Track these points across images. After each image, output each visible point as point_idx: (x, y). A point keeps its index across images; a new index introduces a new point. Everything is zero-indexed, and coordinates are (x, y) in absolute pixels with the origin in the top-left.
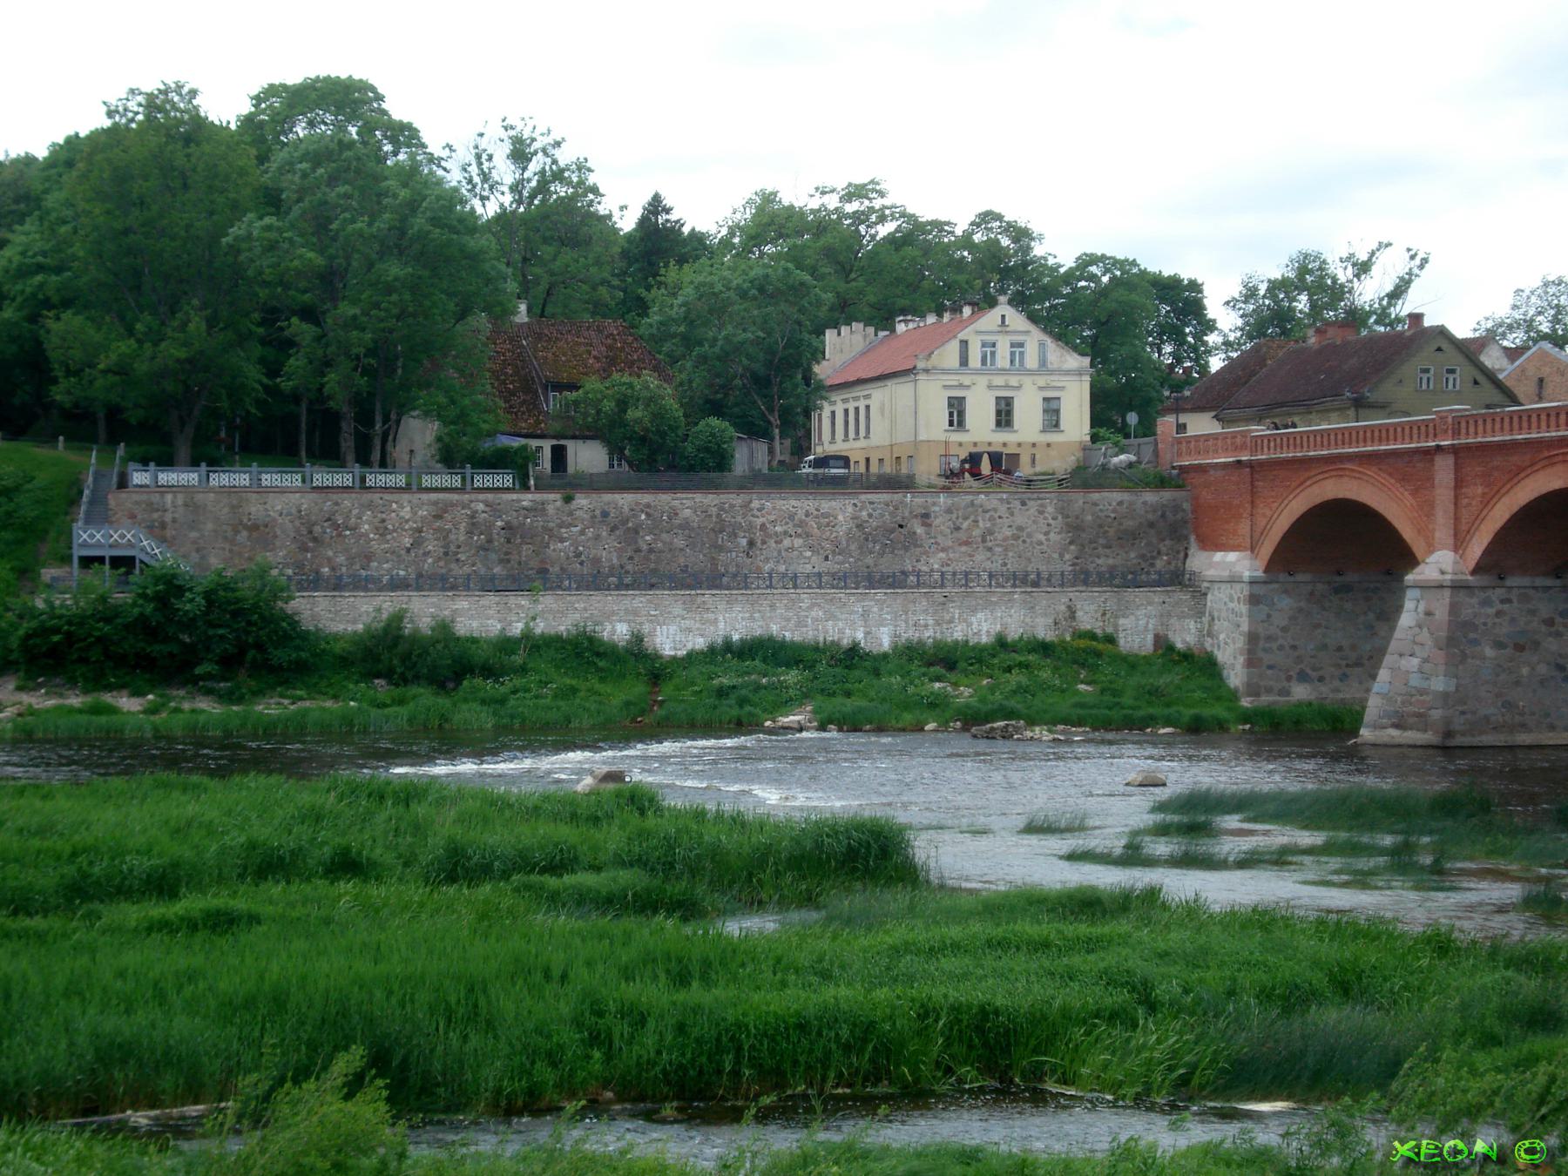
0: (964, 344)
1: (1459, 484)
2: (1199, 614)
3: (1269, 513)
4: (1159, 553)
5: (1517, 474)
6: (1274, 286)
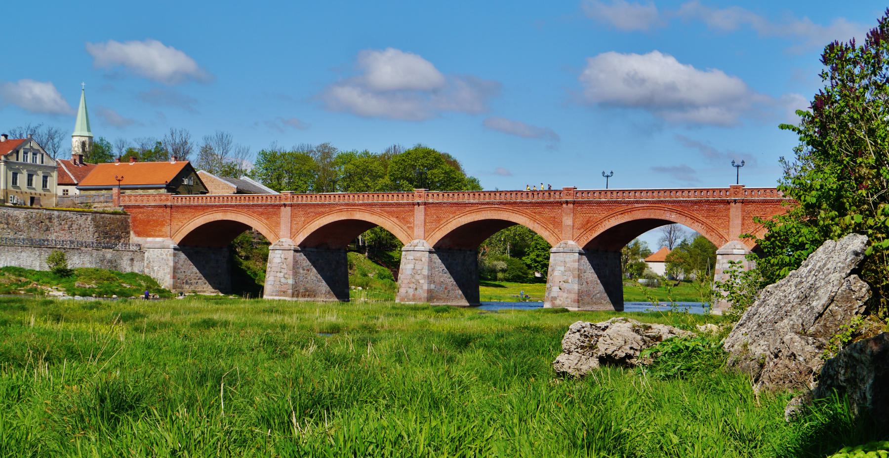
1: (292, 217)
2: (143, 260)
5: (322, 214)
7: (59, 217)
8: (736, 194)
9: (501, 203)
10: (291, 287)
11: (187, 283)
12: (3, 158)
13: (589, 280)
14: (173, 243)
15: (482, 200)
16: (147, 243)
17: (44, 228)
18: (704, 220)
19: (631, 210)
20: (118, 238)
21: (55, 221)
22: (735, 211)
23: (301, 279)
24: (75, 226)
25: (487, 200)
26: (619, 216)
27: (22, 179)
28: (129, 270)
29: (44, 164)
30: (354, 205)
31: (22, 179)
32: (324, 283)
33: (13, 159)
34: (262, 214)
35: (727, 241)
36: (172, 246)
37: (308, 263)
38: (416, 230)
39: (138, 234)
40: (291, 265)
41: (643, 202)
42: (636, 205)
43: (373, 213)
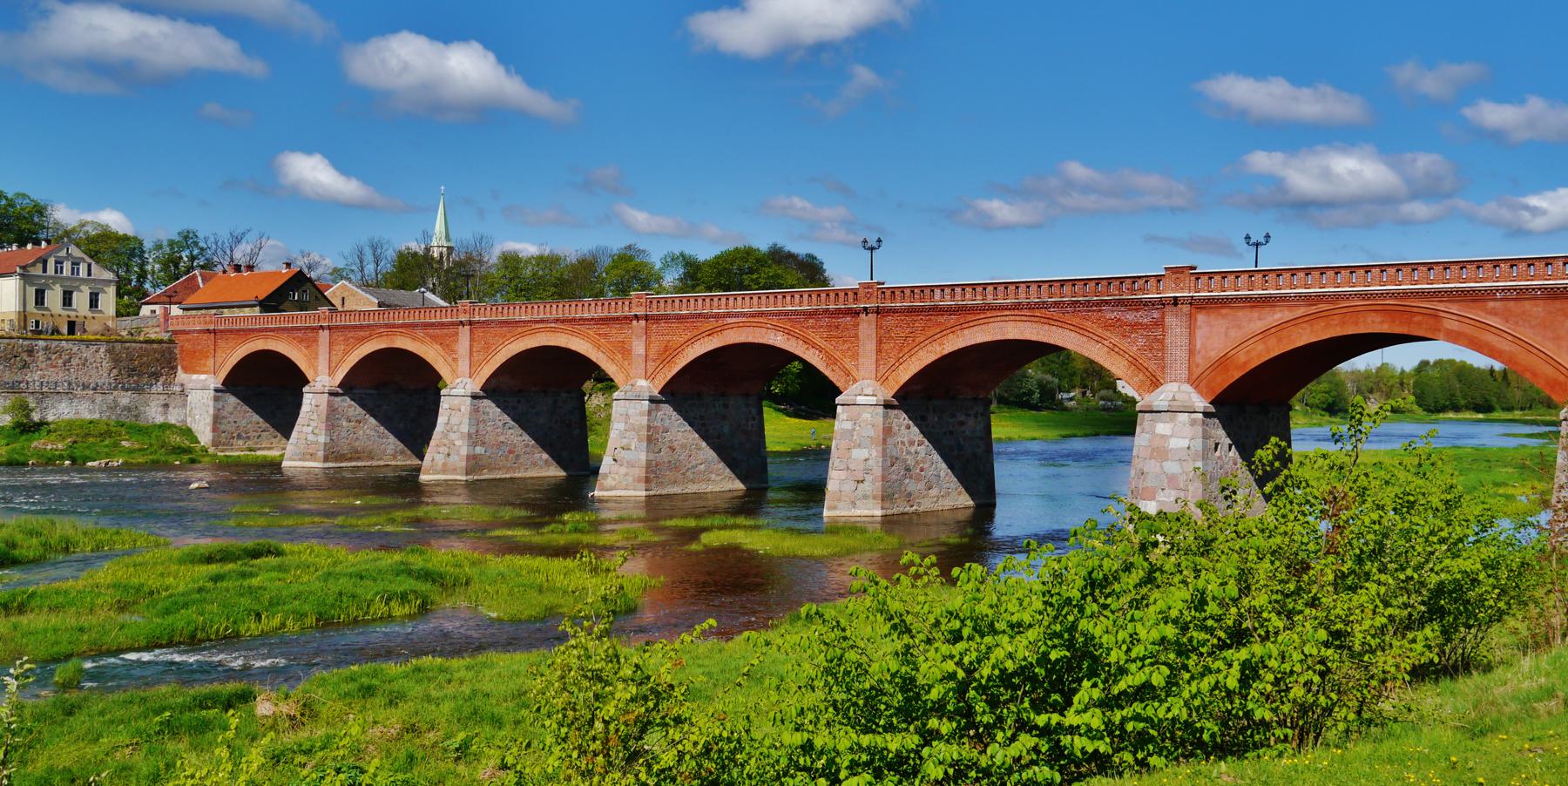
1: (331, 344)
2: (184, 406)
3: (224, 355)
5: (363, 340)
6: (171, 243)
7: (46, 348)
8: (868, 297)
9: (557, 320)
10: (322, 448)
11: (239, 437)
12: (18, 270)
13: (675, 444)
14: (215, 381)
15: (535, 317)
16: (191, 381)
17: (20, 365)
18: (823, 343)
19: (723, 328)
20: (156, 376)
21: (41, 355)
22: (867, 326)
23: (343, 434)
24: (75, 362)
25: (542, 316)
26: (706, 339)
27: (54, 297)
28: (160, 419)
30: (394, 326)
31: (54, 297)
32: (392, 438)
33: (37, 270)
34: (301, 341)
35: (855, 381)
36: (212, 387)
37: (359, 410)
38: (460, 363)
39: (186, 370)
40: (324, 416)
41: (737, 315)
42: (729, 320)
43: (414, 339)
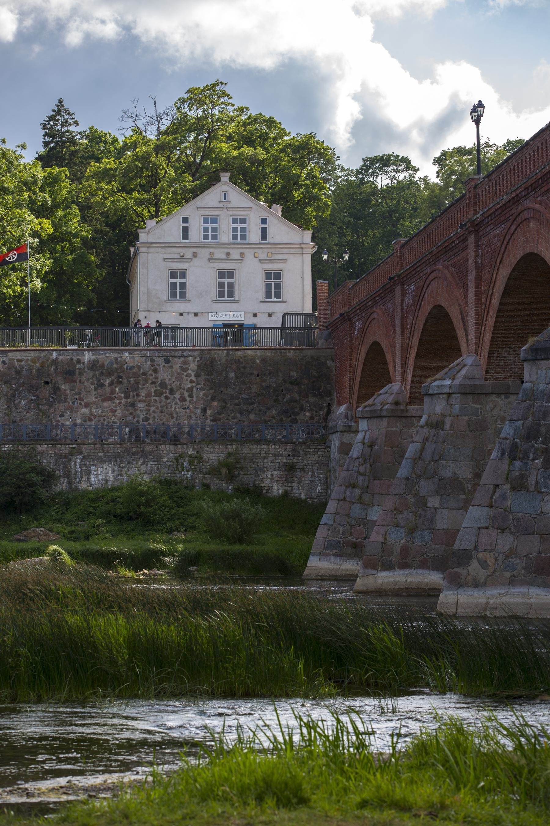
0: (185, 220)
4: (302, 409)
29: (270, 239)
